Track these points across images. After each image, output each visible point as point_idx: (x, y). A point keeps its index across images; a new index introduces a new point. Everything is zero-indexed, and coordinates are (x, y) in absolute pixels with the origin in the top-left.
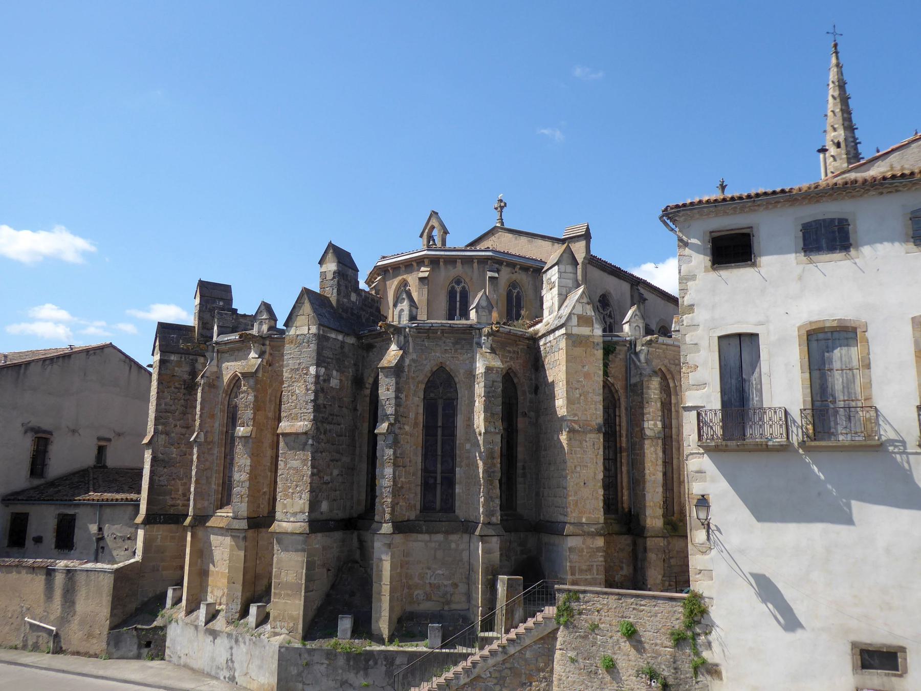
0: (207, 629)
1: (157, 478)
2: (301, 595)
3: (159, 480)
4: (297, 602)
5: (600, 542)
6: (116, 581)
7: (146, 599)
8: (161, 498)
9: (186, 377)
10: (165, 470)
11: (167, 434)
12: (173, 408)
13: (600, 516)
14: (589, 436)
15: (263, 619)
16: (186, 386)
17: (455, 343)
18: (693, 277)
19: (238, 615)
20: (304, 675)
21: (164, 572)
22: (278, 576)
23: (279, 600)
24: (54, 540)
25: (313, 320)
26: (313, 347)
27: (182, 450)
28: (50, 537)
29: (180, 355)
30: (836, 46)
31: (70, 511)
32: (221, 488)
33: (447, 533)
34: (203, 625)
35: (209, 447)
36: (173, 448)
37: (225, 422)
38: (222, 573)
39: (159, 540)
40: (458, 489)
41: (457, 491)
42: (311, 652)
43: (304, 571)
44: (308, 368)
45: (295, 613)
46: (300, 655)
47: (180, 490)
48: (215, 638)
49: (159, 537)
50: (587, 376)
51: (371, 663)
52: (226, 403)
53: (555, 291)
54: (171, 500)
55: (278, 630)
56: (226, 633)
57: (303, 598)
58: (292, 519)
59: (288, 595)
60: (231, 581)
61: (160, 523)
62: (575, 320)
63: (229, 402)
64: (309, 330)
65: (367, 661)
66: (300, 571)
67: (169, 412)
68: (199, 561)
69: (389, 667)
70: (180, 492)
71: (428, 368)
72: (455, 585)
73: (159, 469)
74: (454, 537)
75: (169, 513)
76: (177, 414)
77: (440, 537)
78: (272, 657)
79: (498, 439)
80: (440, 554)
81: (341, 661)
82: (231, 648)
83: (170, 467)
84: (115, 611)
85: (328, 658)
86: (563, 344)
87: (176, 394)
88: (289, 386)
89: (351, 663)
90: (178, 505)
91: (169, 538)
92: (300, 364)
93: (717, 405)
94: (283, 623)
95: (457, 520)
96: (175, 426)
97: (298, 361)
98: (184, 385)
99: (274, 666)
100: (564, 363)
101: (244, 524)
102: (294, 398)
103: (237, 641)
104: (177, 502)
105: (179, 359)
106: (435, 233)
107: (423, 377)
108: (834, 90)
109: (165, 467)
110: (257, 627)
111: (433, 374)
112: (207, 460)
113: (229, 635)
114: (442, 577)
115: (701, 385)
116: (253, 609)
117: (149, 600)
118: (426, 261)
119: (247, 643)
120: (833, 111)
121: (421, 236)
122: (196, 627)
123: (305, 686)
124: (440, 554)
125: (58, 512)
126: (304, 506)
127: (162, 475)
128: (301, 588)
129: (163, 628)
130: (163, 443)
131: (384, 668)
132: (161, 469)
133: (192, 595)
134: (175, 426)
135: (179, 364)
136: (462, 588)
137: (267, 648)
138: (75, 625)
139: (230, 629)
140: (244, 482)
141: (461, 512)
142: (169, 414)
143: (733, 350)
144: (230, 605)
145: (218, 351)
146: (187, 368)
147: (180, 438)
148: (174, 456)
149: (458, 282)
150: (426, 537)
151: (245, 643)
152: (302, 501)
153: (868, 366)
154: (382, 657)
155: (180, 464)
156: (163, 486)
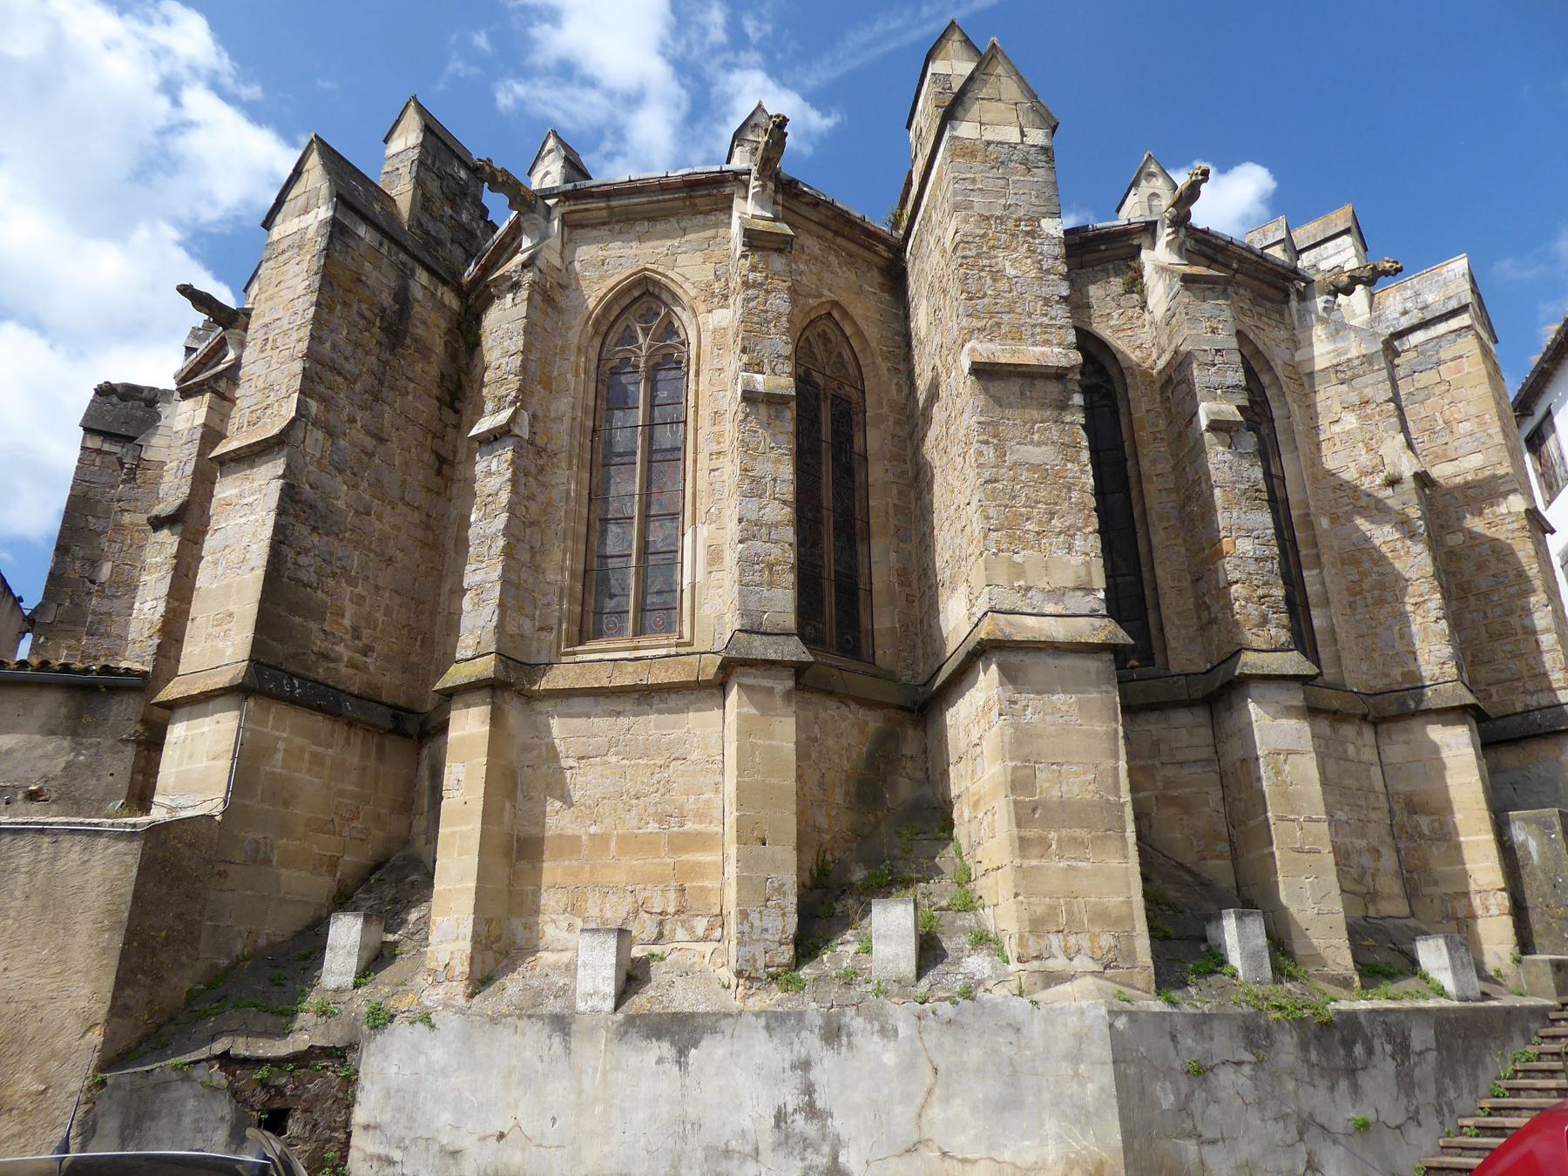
0: (631, 1021)
1: (291, 554)
2: (1124, 839)
3: (295, 563)
4: (1115, 862)
6: (147, 868)
7: (223, 962)
8: (298, 620)
9: (386, 299)
10: (315, 538)
11: (330, 433)
12: (349, 366)
15: (929, 951)
16: (385, 324)
19: (787, 953)
20: (1196, 1106)
21: (285, 872)
23: (1043, 862)
25: (1031, 116)
27: (360, 498)
29: (378, 236)
32: (579, 587)
34: (610, 1004)
35: (540, 462)
36: (339, 479)
37: (592, 404)
38: (622, 839)
39: (279, 756)
41: (1316, 623)
42: (1201, 1022)
43: (1123, 765)
44: (1034, 220)
45: (1114, 901)
46: (1174, 1038)
47: (347, 614)
48: (682, 1052)
49: (281, 745)
51: (1358, 1050)
52: (593, 355)
54: (323, 636)
55: (1058, 964)
56: (757, 1015)
57: (1133, 851)
58: (1050, 608)
59: (1074, 841)
60: (752, 836)
61: (292, 701)
63: (600, 353)
64: (1023, 134)
65: (1348, 1045)
66: (1108, 764)
67: (340, 374)
68: (508, 806)
69: (1403, 1062)
70: (347, 622)
72: (1375, 852)
73: (299, 526)
74: (1348, 731)
75: (312, 675)
76: (358, 387)
78: (1075, 1058)
81: (1287, 1048)
82: (805, 1065)
83: (327, 535)
84: (128, 992)
85: (1251, 1045)
87: (361, 332)
88: (979, 256)
89: (1314, 1057)
90: (337, 660)
91: (307, 756)
92: (1006, 207)
94: (1072, 940)
96: (352, 420)
97: (1003, 201)
98: (382, 318)
99: (1099, 1081)
101: (794, 650)
102: (1003, 285)
103: (833, 1033)
104: (337, 648)
105: (376, 244)
109: (314, 529)
110: (919, 976)
112: (532, 497)
113: (775, 1022)
114: (1346, 826)
117: (231, 967)
119: (903, 1030)
122: (562, 1024)
123: (1206, 1149)
126: (1089, 573)
127: (306, 551)
128: (1121, 818)
129: (341, 1055)
130: (318, 455)
131: (1390, 1066)
132: (305, 530)
133: (489, 921)
134: (352, 420)
136: (1389, 861)
137: (1036, 1029)
139: (770, 999)
140: (776, 525)
142: (340, 380)
144: (754, 917)
145: (563, 222)
147: (359, 461)
148: (340, 504)
151: (887, 1032)
152: (1076, 560)
154: (1379, 1030)
155: (354, 537)
156: (305, 585)
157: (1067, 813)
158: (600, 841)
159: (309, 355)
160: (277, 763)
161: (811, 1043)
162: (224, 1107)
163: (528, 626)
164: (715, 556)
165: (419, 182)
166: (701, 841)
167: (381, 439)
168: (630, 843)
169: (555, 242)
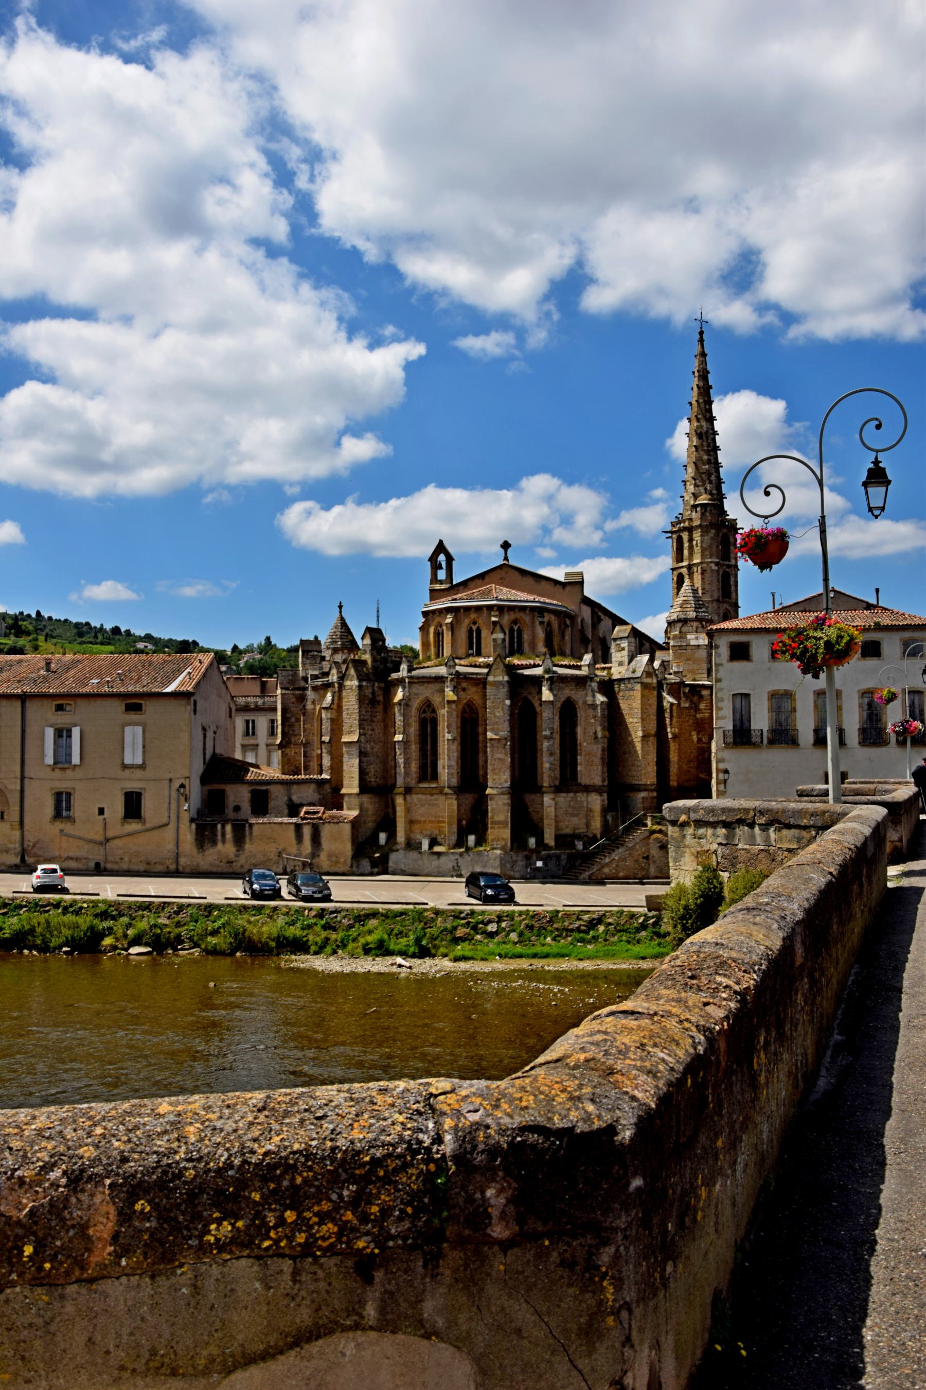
5: (655, 794)
9: (370, 696)
11: (365, 735)
13: (655, 780)
14: (651, 738)
17: (576, 685)
18: (721, 665)
22: (492, 818)
24: (250, 808)
26: (506, 689)
28: (246, 808)
30: (701, 333)
31: (264, 788)
33: (576, 792)
40: (579, 768)
45: (505, 836)
50: (650, 705)
53: (625, 653)
60: (450, 824)
62: (645, 674)
71: (562, 700)
74: (579, 794)
77: (572, 795)
79: (606, 741)
80: (572, 803)
86: (638, 687)
93: (731, 728)
95: (580, 785)
100: (639, 698)
106: (442, 558)
107: (558, 705)
108: (699, 380)
111: (564, 702)
115: (723, 718)
116: (472, 839)
118: (495, 608)
120: (697, 401)
121: (430, 560)
124: (572, 803)
125: (251, 788)
135: (367, 687)
138: (323, 856)
141: (583, 779)
143: (738, 700)
146: (370, 690)
149: (515, 622)
150: (565, 795)
153: (795, 711)
157: (499, 823)
158: (425, 821)
159: (360, 720)
160: (365, 805)
161: (457, 857)
162: (368, 864)
163: (409, 780)
164: (444, 767)
165: (372, 655)
166: (443, 822)
167: (373, 730)
168: (430, 822)
169: (407, 689)
